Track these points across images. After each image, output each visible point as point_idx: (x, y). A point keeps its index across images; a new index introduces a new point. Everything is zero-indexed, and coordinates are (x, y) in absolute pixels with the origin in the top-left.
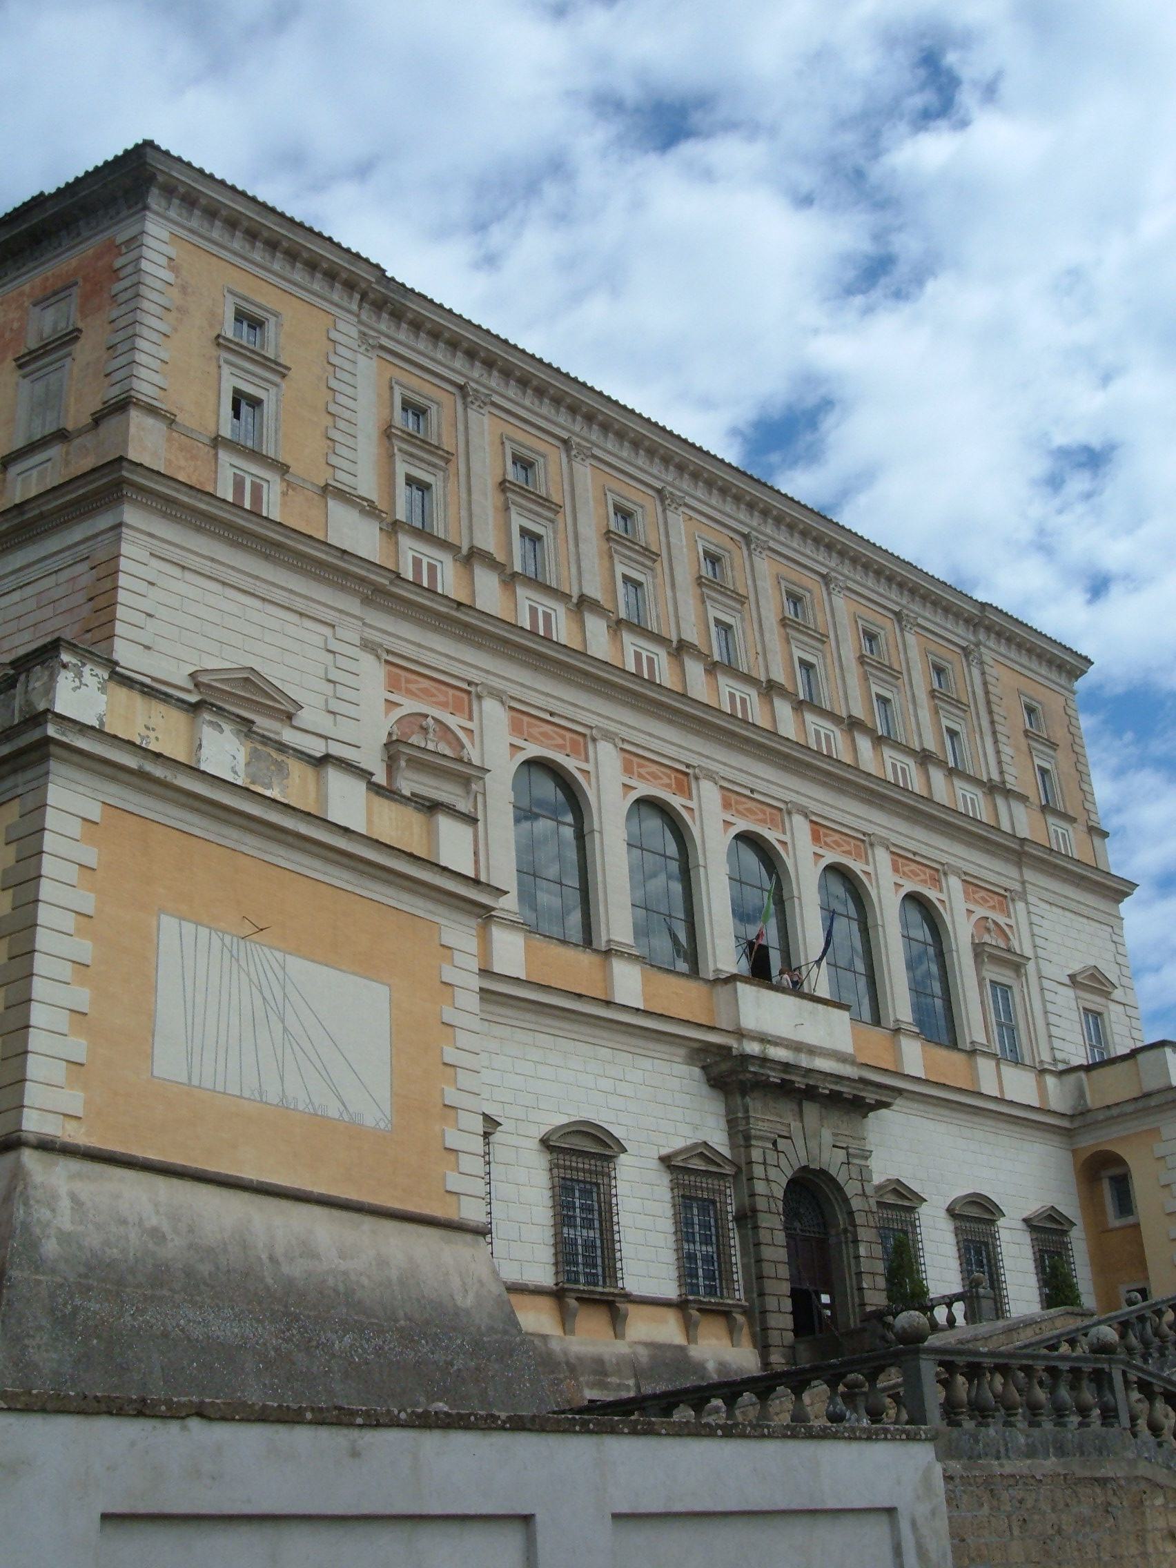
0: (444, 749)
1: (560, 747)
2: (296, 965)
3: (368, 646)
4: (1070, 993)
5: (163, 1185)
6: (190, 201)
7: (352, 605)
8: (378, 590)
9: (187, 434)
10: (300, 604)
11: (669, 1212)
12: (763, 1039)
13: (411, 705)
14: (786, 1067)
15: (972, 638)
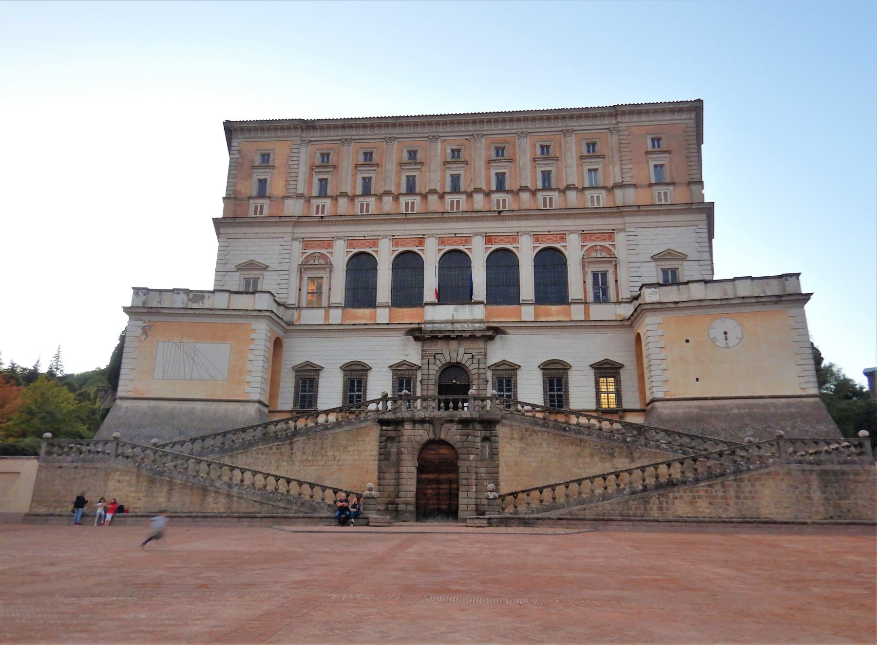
0: (322, 262)
1: (367, 247)
2: (199, 345)
3: (293, 239)
4: (653, 264)
5: (152, 403)
6: (242, 130)
7: (289, 229)
8: (296, 222)
9: (241, 200)
10: (272, 236)
11: (391, 383)
12: (433, 323)
13: (310, 252)
14: (432, 332)
15: (614, 122)
